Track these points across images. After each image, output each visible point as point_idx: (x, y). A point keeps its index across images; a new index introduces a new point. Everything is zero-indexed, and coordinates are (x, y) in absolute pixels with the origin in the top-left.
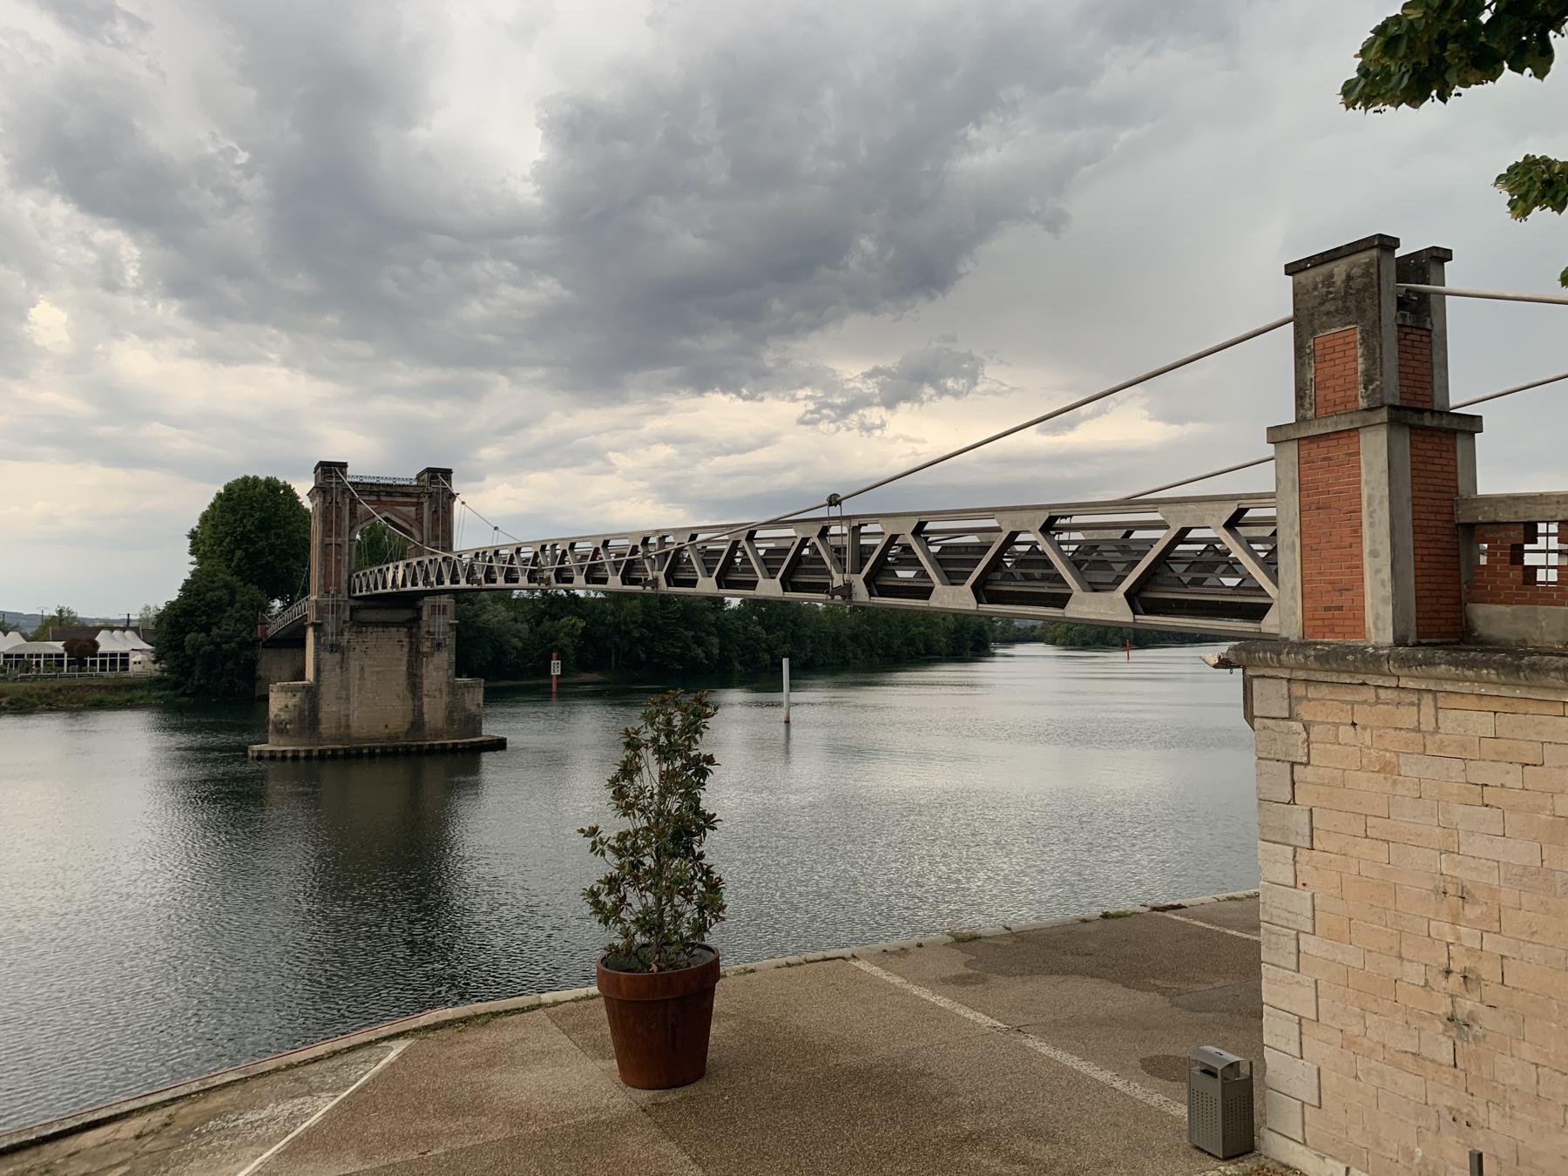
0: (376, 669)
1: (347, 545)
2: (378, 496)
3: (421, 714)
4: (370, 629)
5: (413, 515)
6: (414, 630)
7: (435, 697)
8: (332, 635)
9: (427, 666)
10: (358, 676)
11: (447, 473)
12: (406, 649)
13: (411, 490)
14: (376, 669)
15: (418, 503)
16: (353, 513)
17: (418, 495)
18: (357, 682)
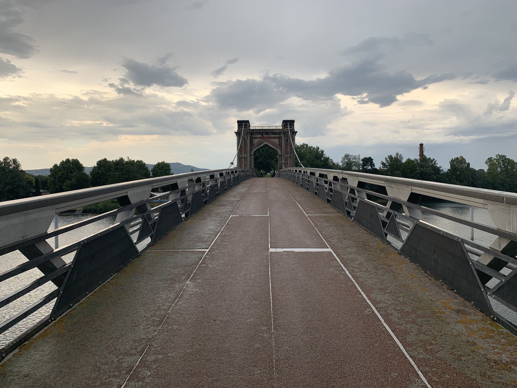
1: (249, 158)
2: (262, 135)
5: (277, 143)
11: (292, 122)
13: (276, 131)
15: (279, 137)
16: (251, 143)
17: (280, 133)
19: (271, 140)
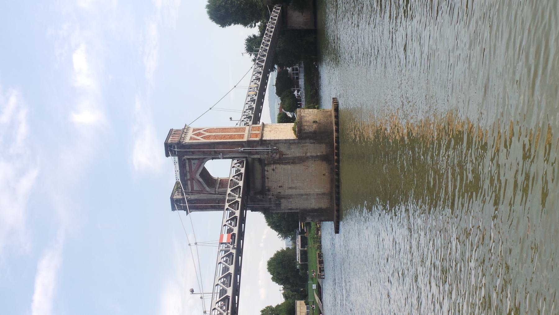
0: (290, 181)
2: (187, 180)
3: (317, 156)
4: (266, 185)
5: (196, 161)
6: (266, 162)
7: (307, 149)
8: (271, 204)
9: (288, 154)
10: (294, 190)
12: (278, 166)
14: (290, 181)
18: (298, 190)
19: (193, 170)
